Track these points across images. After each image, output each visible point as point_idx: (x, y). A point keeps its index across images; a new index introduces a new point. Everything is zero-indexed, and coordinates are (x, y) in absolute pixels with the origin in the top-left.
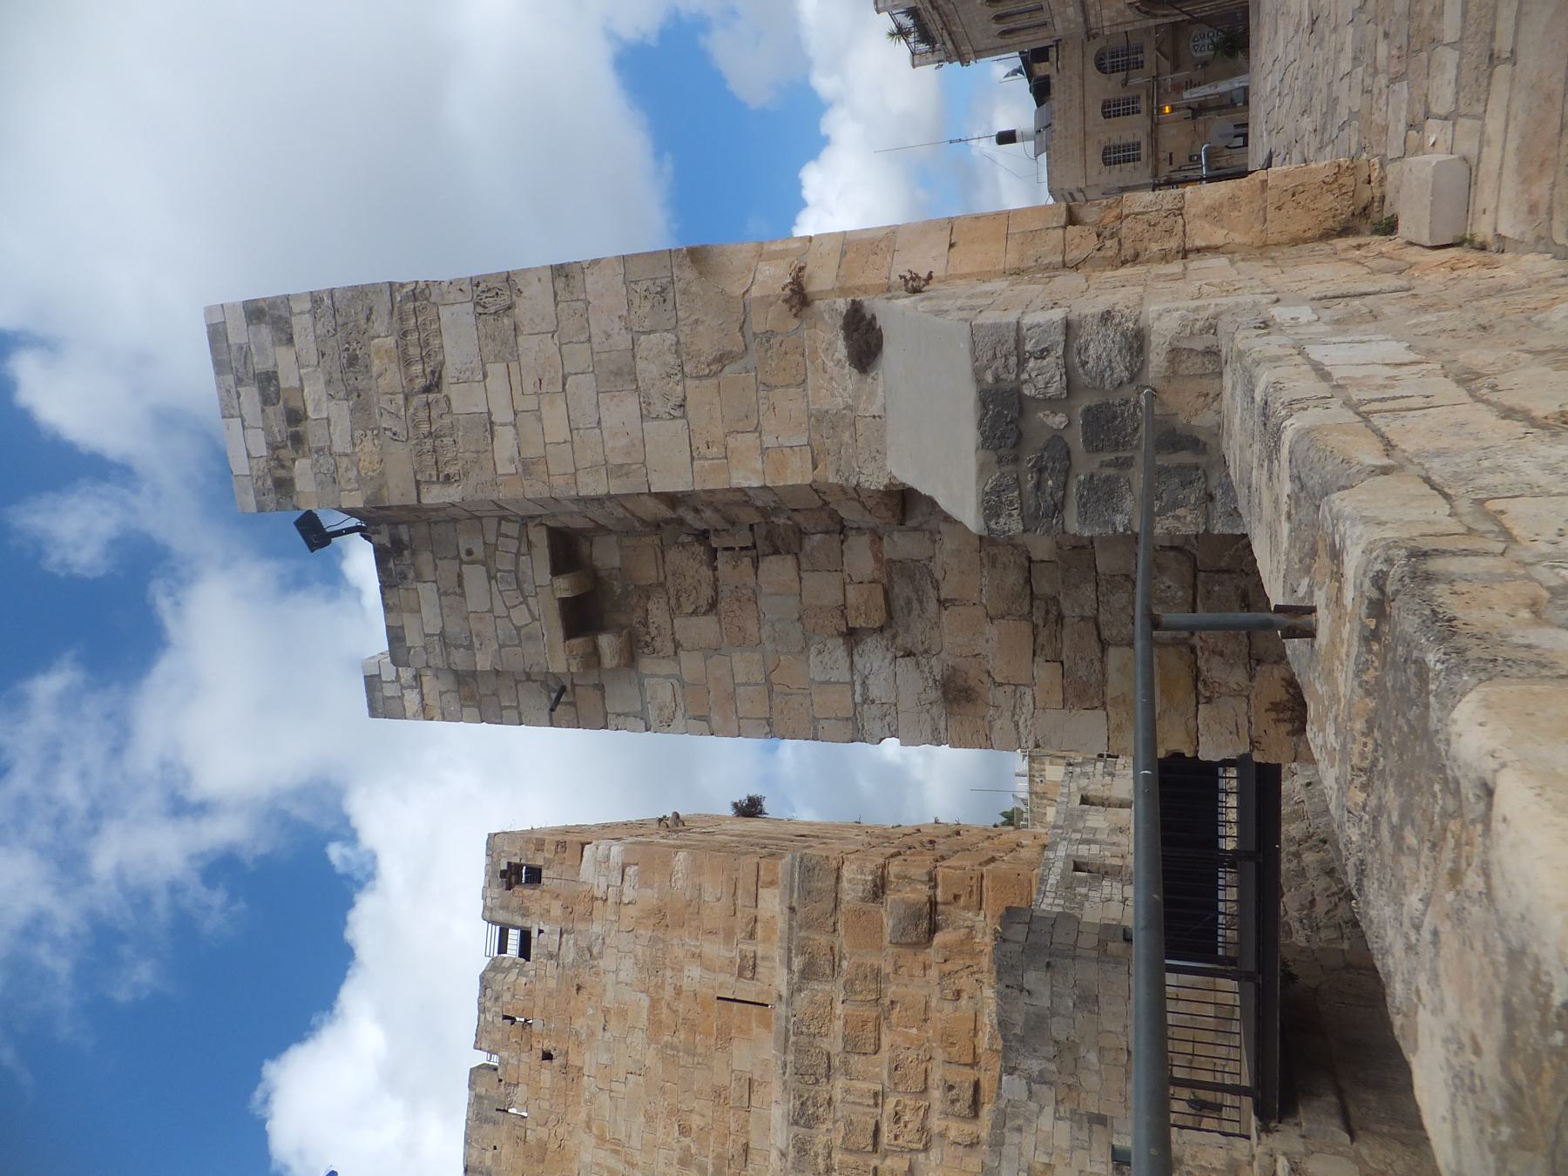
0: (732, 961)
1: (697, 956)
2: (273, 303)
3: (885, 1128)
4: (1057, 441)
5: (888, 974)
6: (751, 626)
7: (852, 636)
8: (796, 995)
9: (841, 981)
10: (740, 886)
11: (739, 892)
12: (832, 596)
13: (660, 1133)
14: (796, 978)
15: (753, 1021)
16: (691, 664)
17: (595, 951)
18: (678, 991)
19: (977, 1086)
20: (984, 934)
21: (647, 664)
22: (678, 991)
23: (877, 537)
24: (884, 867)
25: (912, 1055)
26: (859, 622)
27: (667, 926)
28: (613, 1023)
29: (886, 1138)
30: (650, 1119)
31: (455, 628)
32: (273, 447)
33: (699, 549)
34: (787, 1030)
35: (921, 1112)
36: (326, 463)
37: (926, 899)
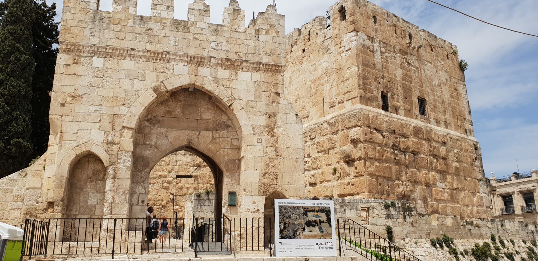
5: (334, 151)
8: (326, 123)
9: (331, 136)
10: (351, 93)
11: (349, 94)
15: (320, 111)
17: (328, 52)
20: (349, 179)
22: (323, 85)
24: (361, 142)
25: (319, 163)
27: (337, 73)
28: (313, 67)
34: (318, 123)
35: (308, 169)
37: (353, 157)
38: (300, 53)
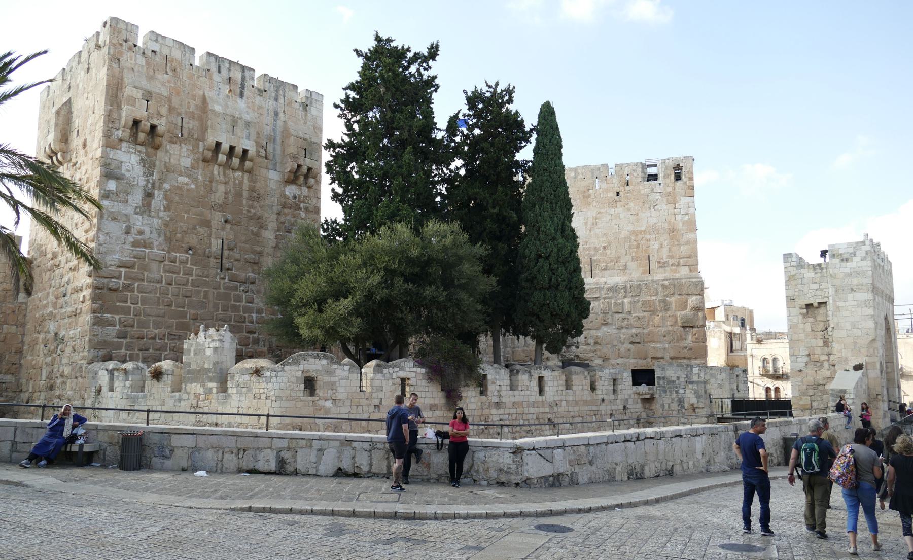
0: (662, 259)
1: (661, 246)
3: (620, 315)
6: (810, 338)
7: (809, 355)
12: (816, 352)
13: (601, 240)
14: (661, 282)
16: (802, 326)
18: (649, 240)
19: (639, 343)
21: (801, 317)
22: (649, 240)
23: (828, 360)
26: (812, 357)
28: (635, 217)
29: (617, 315)
30: (605, 235)
31: (805, 281)
32: (841, 254)
33: (824, 329)
36: (838, 266)
38: (612, 194)
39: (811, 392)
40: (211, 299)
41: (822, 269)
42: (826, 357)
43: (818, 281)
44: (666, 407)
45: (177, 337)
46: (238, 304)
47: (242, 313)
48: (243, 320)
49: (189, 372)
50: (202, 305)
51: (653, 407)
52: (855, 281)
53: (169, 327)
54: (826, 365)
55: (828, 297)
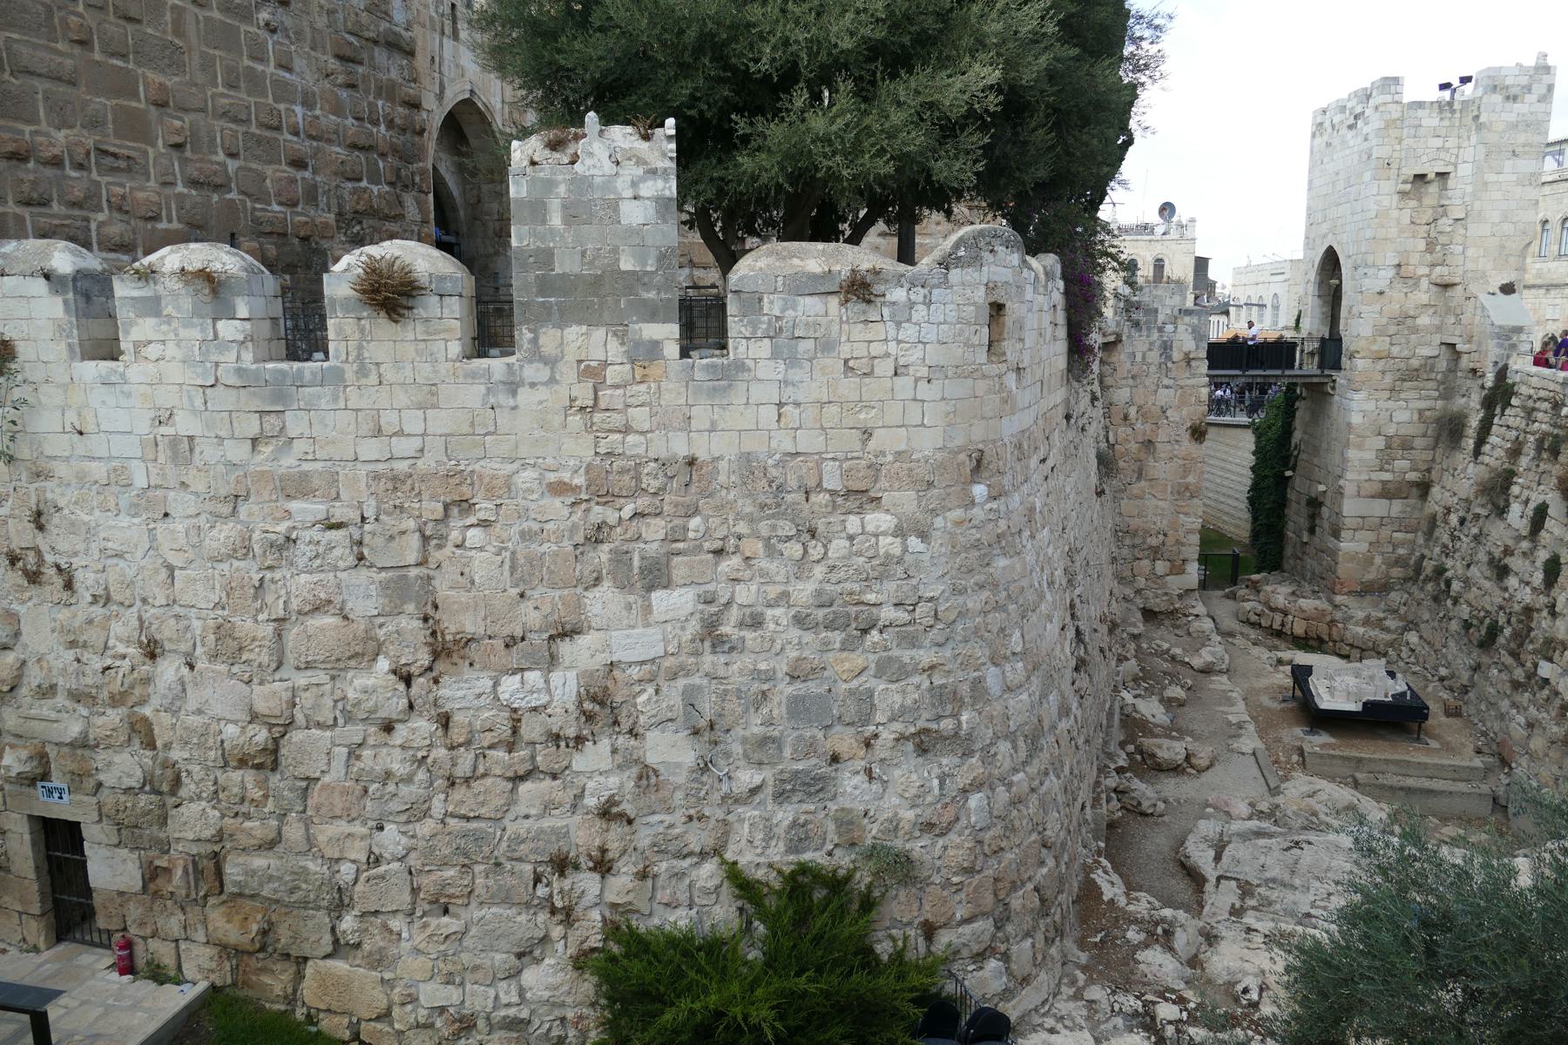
2: (1551, 97)
4: (1510, 339)
7: (1399, 265)
16: (1395, 213)
21: (1396, 197)
23: (1427, 276)
26: (1403, 268)
31: (1422, 131)
32: (1507, 87)
39: (1392, 329)
40: (194, 40)
41: (1453, 112)
42: (1425, 270)
43: (1443, 135)
44: (1139, 358)
45: (122, 164)
46: (260, 68)
47: (270, 100)
48: (275, 123)
49: (545, 286)
50: (173, 58)
51: (1114, 359)
52: (1522, 138)
53: (94, 124)
54: (1424, 283)
55: (1455, 165)
